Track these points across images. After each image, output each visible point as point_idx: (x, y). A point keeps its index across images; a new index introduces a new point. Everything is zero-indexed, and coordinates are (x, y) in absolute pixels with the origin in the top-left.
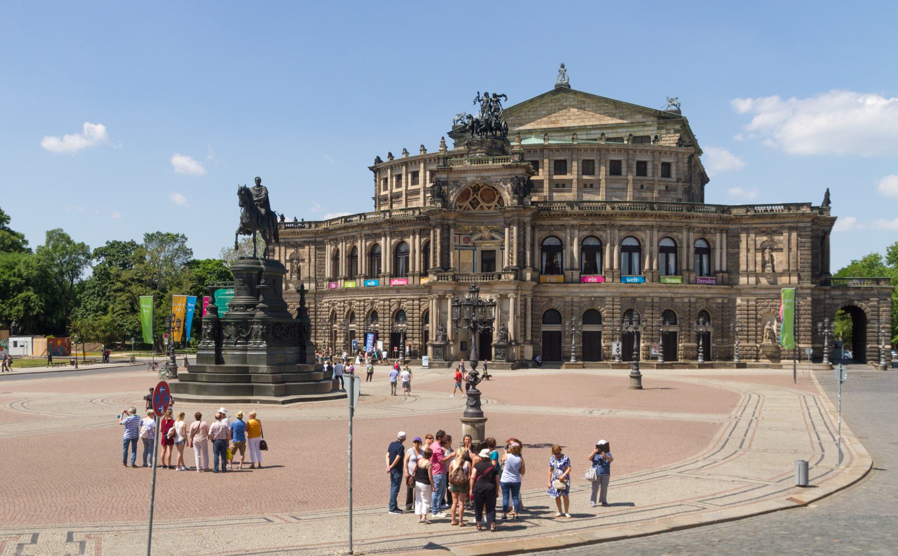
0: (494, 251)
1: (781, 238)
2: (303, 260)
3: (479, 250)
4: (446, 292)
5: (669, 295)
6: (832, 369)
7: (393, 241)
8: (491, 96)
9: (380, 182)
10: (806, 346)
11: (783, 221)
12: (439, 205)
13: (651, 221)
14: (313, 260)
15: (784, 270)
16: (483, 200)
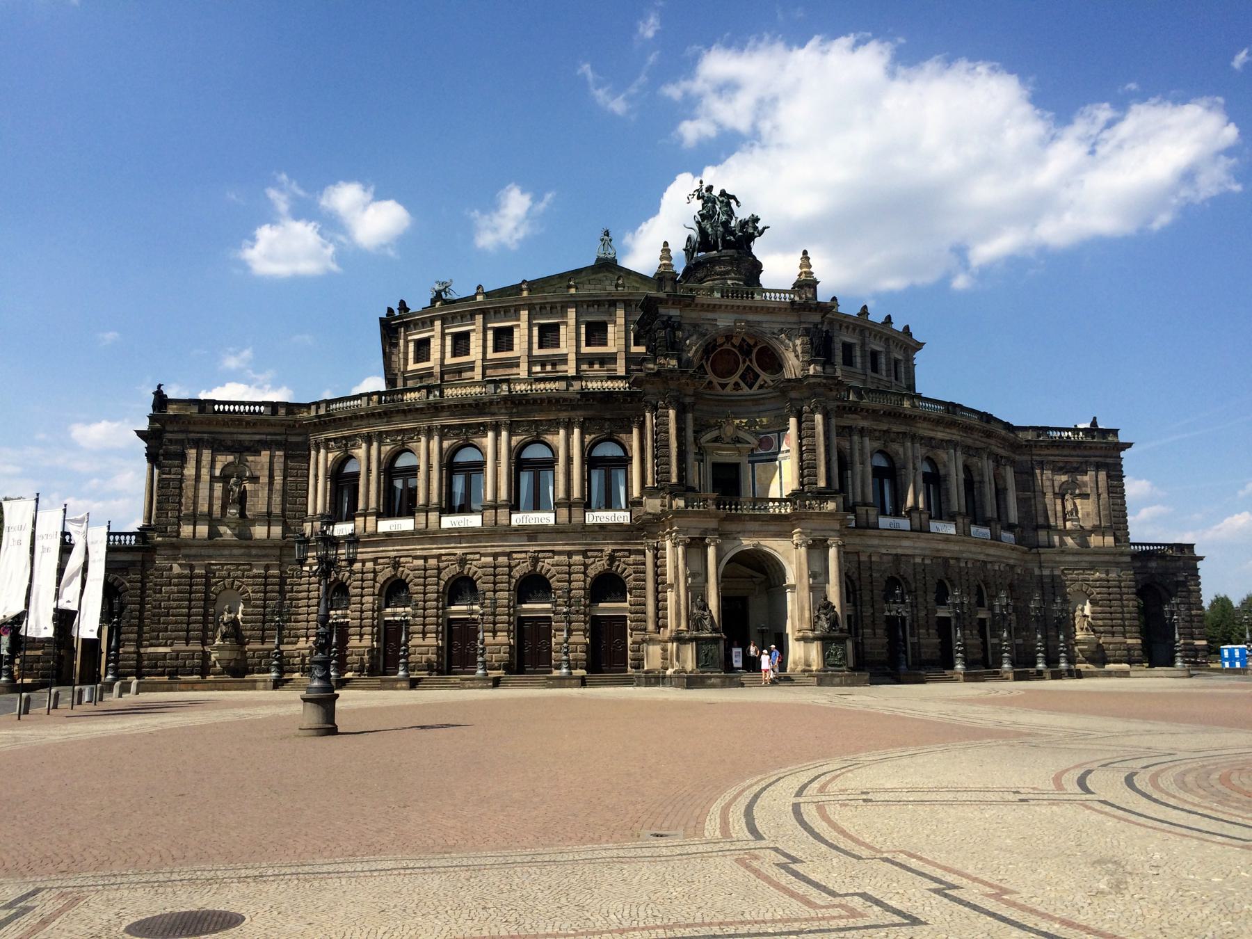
0: (736, 467)
1: (1086, 478)
2: (254, 479)
3: (710, 459)
4: (706, 531)
5: (982, 557)
6: (1191, 676)
7: (515, 440)
8: (716, 192)
9: (406, 347)
10: (1134, 641)
11: (1086, 453)
12: (674, 362)
13: (955, 435)
14: (278, 479)
15: (1094, 526)
16: (714, 371)
